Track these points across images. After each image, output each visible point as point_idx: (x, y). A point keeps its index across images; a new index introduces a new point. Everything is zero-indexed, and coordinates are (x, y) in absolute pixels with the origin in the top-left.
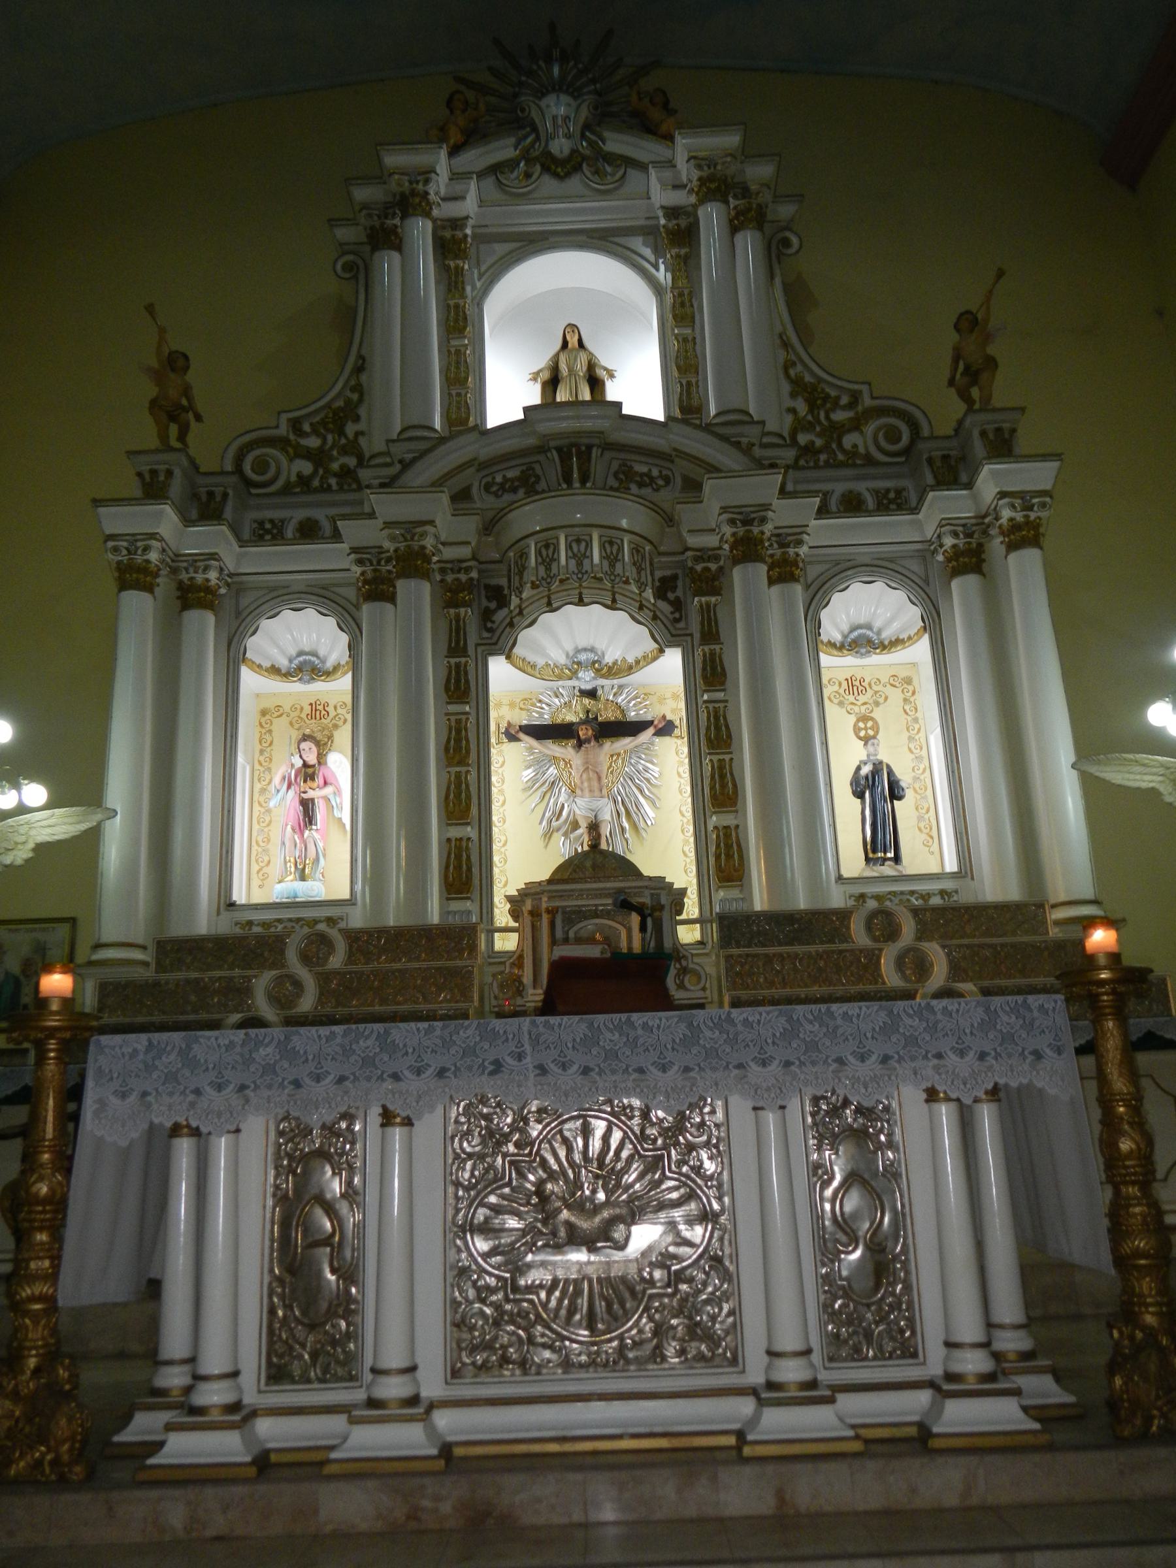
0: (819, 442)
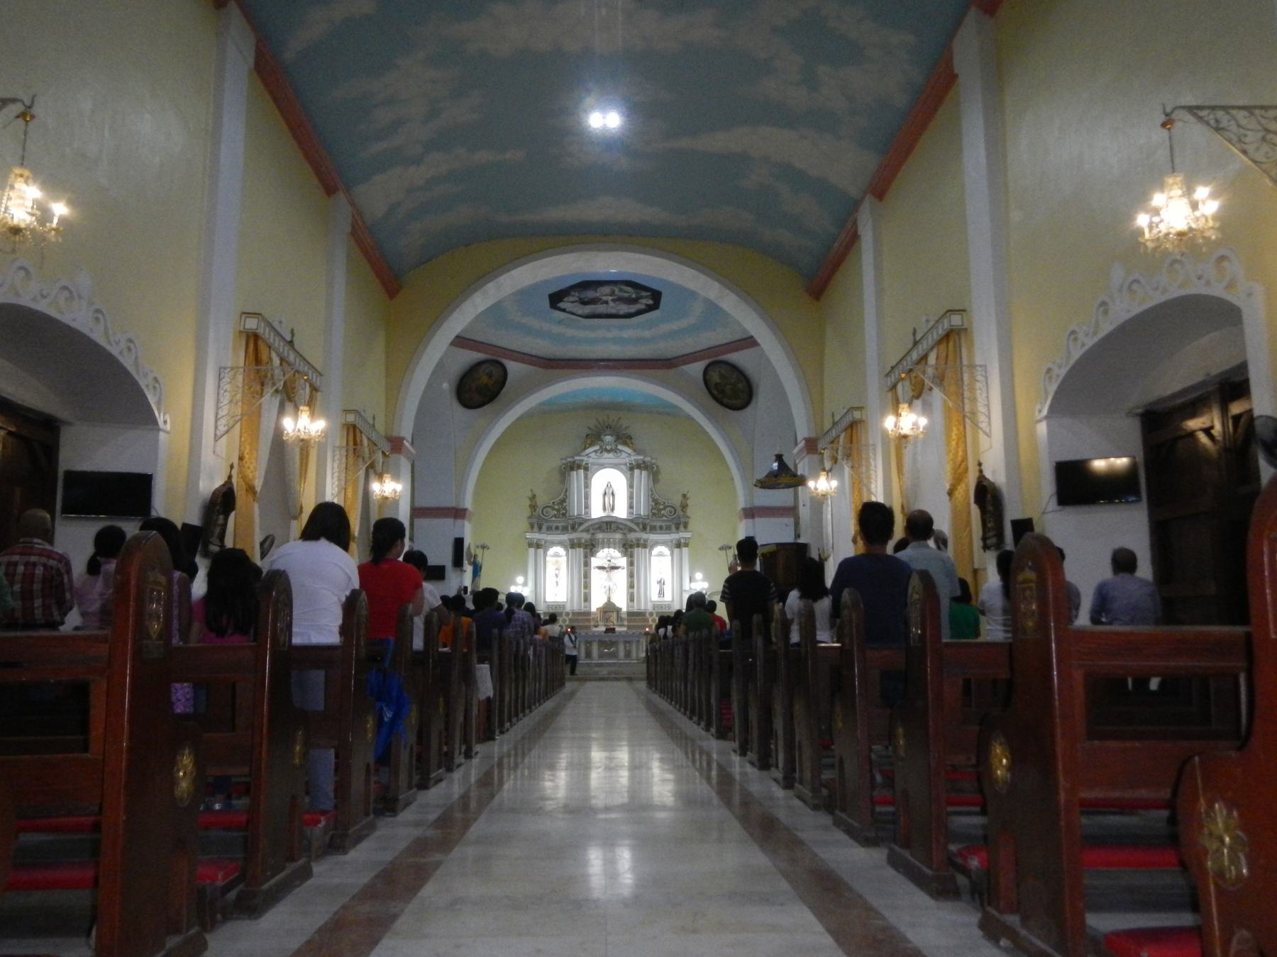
0: (657, 512)
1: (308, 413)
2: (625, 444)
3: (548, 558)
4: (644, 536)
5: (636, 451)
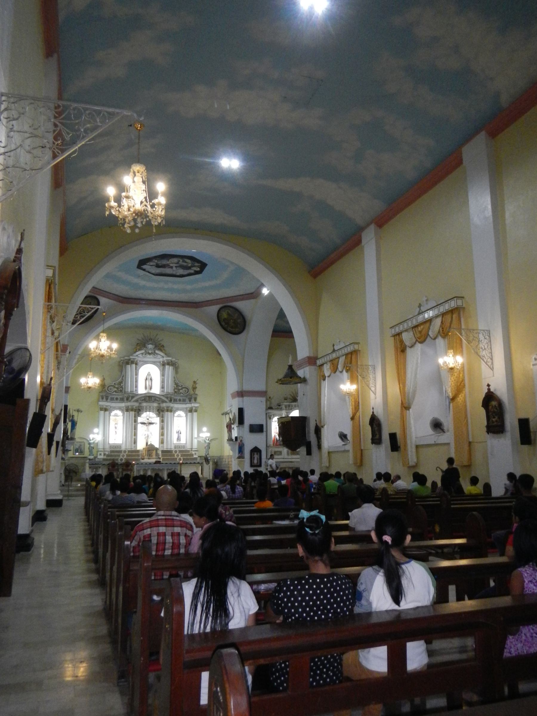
0: (177, 391)
1: (106, 338)
2: (161, 350)
3: (111, 417)
4: (171, 405)
5: (167, 355)
